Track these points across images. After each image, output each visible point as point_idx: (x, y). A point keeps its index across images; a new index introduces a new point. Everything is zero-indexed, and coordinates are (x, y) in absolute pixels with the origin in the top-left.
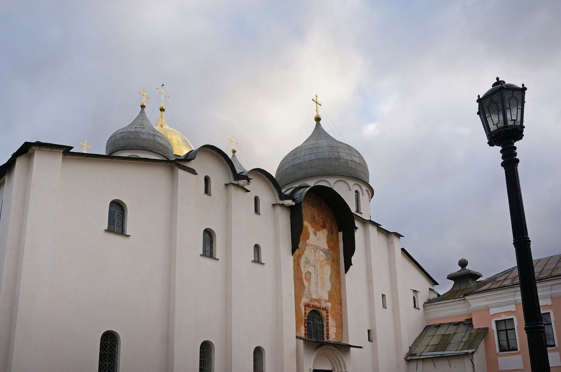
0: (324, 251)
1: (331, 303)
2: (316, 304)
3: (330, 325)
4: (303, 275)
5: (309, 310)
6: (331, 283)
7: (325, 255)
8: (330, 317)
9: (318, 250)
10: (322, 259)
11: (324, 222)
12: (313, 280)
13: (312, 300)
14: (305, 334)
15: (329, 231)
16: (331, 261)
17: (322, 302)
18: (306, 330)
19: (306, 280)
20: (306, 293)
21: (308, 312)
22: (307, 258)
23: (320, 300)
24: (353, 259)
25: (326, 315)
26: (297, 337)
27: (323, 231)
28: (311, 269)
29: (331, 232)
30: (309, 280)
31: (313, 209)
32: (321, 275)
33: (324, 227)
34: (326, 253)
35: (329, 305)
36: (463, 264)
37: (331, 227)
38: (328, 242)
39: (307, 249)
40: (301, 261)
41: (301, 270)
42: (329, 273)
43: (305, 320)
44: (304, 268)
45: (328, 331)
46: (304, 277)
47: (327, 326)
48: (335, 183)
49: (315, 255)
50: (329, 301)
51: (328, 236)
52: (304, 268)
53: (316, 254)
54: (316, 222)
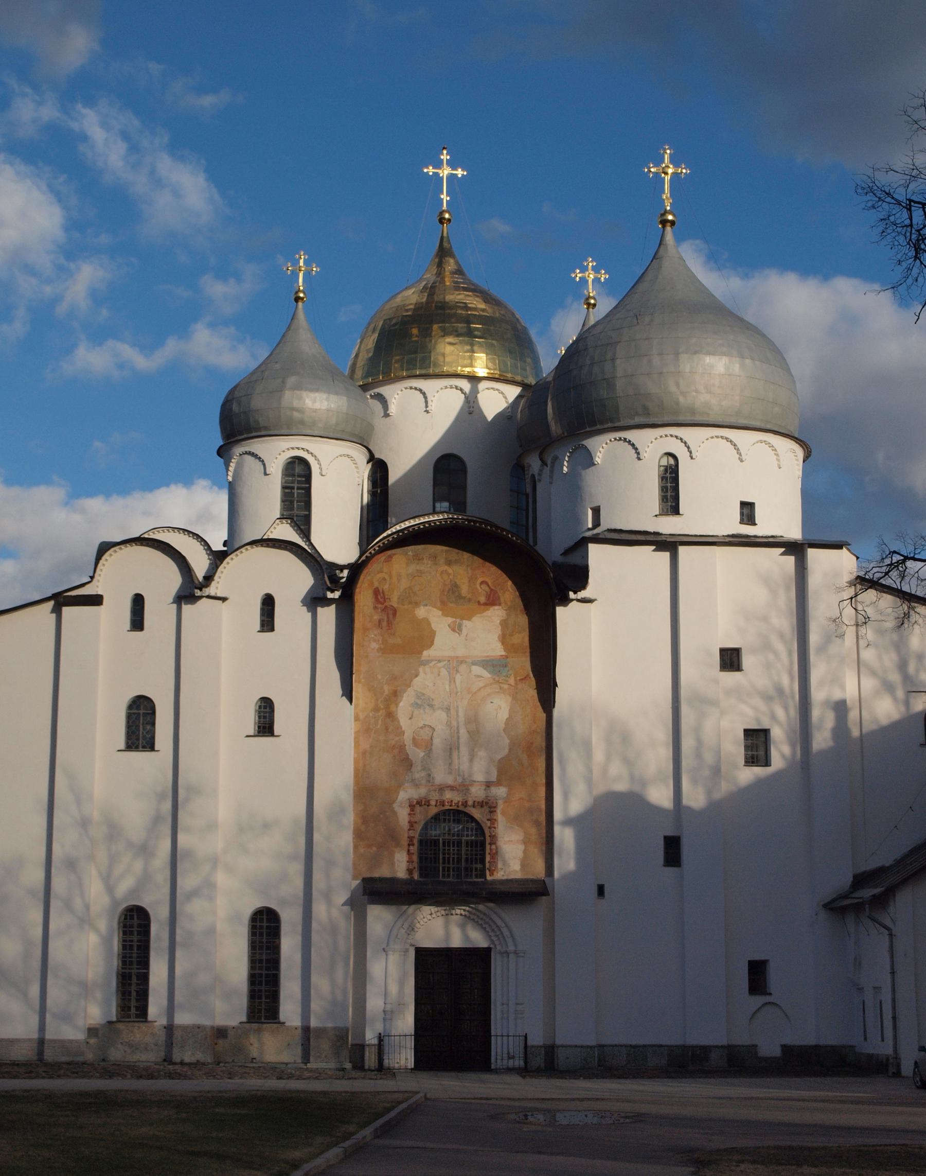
0: (489, 664)
7: (490, 673)
9: (463, 668)
10: (481, 684)
14: (410, 871)
15: (510, 609)
16: (512, 681)
23: (464, 786)
31: (450, 571)
33: (492, 601)
38: (503, 639)
39: (422, 674)
40: (401, 704)
41: (399, 727)
44: (410, 719)
49: (452, 680)
53: (458, 678)
54: (460, 597)
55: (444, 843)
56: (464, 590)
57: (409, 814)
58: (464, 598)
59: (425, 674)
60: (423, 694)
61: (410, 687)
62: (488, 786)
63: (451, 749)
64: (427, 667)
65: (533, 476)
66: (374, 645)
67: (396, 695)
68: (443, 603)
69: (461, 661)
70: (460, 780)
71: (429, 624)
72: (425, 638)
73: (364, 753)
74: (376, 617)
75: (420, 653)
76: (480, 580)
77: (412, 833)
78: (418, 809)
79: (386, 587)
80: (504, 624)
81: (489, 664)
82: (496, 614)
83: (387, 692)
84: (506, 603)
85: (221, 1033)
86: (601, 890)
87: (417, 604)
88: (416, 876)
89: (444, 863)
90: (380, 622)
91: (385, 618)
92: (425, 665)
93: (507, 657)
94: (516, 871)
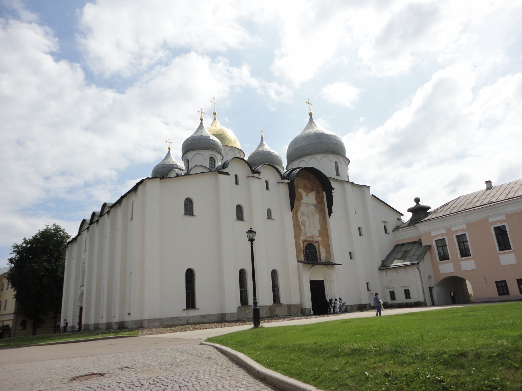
0: (314, 205)
1: (321, 237)
2: (310, 239)
3: (321, 252)
5: (305, 244)
6: (320, 225)
8: (321, 247)
10: (313, 211)
12: (307, 224)
14: (304, 259)
15: (316, 192)
16: (319, 211)
17: (315, 238)
18: (305, 256)
19: (303, 225)
21: (305, 245)
22: (302, 212)
24: (334, 208)
25: (318, 245)
26: (298, 261)
27: (312, 193)
28: (306, 218)
29: (318, 193)
30: (304, 225)
33: (313, 190)
34: (315, 206)
35: (320, 239)
36: (417, 200)
37: (318, 189)
40: (298, 214)
42: (318, 219)
43: (304, 250)
44: (301, 218)
45: (320, 255)
46: (301, 224)
47: (319, 252)
48: (321, 158)
49: (308, 209)
50: (319, 237)
51: (316, 196)
69: (309, 204)
70: (312, 235)
75: (301, 201)
76: (310, 184)
78: (304, 242)
93: (317, 204)
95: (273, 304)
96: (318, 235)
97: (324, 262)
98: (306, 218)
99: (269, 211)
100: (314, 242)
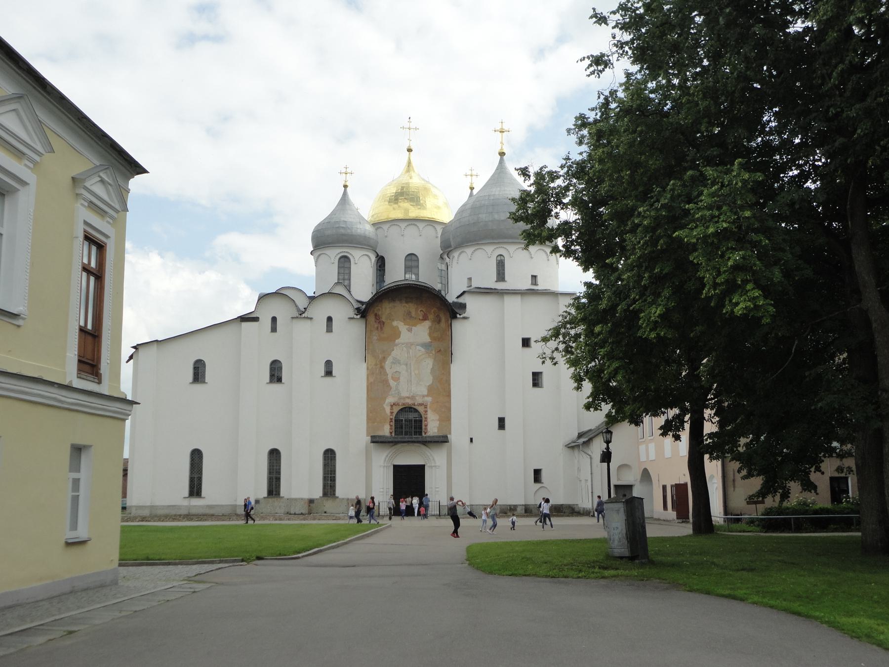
0: (424, 345)
4: (389, 376)
10: (421, 354)
11: (425, 314)
13: (400, 398)
14: (391, 433)
15: (433, 321)
16: (434, 353)
17: (417, 398)
20: (393, 393)
30: (397, 379)
31: (407, 306)
32: (417, 372)
33: (425, 318)
35: (429, 399)
38: (430, 334)
40: (387, 362)
42: (430, 366)
44: (391, 369)
45: (426, 426)
49: (408, 352)
50: (427, 396)
52: (391, 369)
53: (411, 351)
54: (411, 317)
55: (405, 421)
56: (413, 314)
57: (391, 409)
58: (413, 317)
59: (397, 349)
60: (396, 358)
61: (390, 355)
62: (424, 397)
63: (408, 381)
64: (398, 347)
65: (447, 263)
66: (375, 338)
67: (384, 359)
68: (404, 319)
69: (412, 344)
70: (412, 394)
71: (398, 328)
72: (397, 334)
73: (371, 383)
74: (376, 326)
76: (420, 310)
77: (391, 417)
78: (394, 407)
79: (380, 313)
80: (430, 328)
81: (424, 345)
82: (427, 324)
83: (380, 357)
84: (431, 319)
85: (311, 501)
86: (471, 440)
87: (393, 320)
88: (393, 434)
89: (405, 429)
90: (377, 328)
91: (380, 326)
92: (396, 346)
94: (435, 432)
95: (320, 497)
96: (425, 393)
97: (433, 437)
98: (402, 369)
99: (329, 364)
100: (415, 405)
